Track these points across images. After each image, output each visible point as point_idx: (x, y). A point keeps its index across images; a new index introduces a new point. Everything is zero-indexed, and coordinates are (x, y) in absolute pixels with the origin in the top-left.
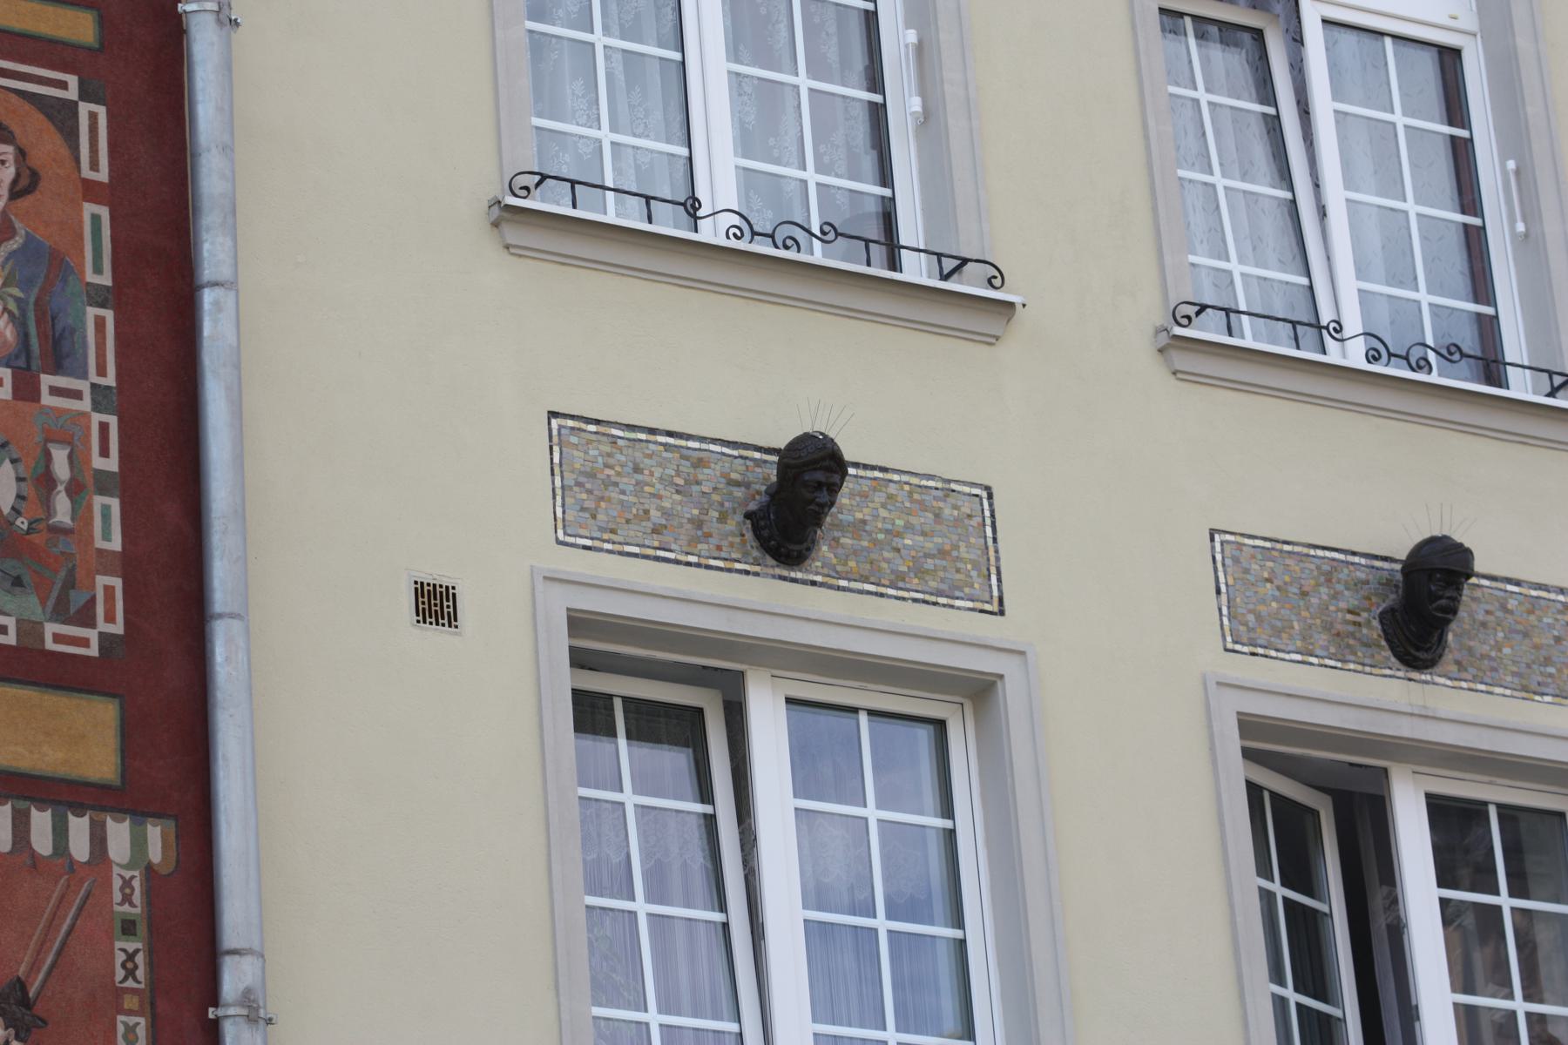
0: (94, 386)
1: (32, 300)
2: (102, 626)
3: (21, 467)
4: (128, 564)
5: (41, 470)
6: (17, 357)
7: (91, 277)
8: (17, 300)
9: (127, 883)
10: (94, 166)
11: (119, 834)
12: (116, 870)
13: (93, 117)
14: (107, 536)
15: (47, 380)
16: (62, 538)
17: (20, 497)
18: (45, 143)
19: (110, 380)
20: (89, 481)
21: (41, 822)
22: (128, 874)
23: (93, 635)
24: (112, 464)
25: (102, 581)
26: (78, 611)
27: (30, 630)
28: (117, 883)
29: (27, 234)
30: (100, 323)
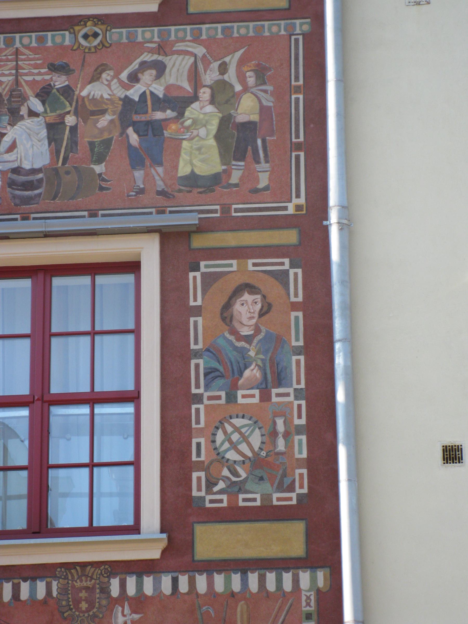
0: (295, 390)
1: (268, 358)
2: (298, 491)
3: (263, 430)
4: (310, 463)
5: (272, 430)
6: (261, 384)
7: (294, 343)
8: (262, 360)
9: (308, 598)
10: (296, 295)
11: (305, 577)
12: (303, 593)
13: (296, 274)
14: (300, 452)
15: (274, 391)
16: (281, 456)
17: (263, 443)
18: (273, 289)
19: (303, 386)
20: (293, 430)
21: (271, 577)
22: (308, 594)
23: (294, 495)
24: (303, 421)
25: (298, 471)
26: (288, 486)
27: (266, 498)
28: (304, 598)
29: (266, 331)
30: (298, 362)
